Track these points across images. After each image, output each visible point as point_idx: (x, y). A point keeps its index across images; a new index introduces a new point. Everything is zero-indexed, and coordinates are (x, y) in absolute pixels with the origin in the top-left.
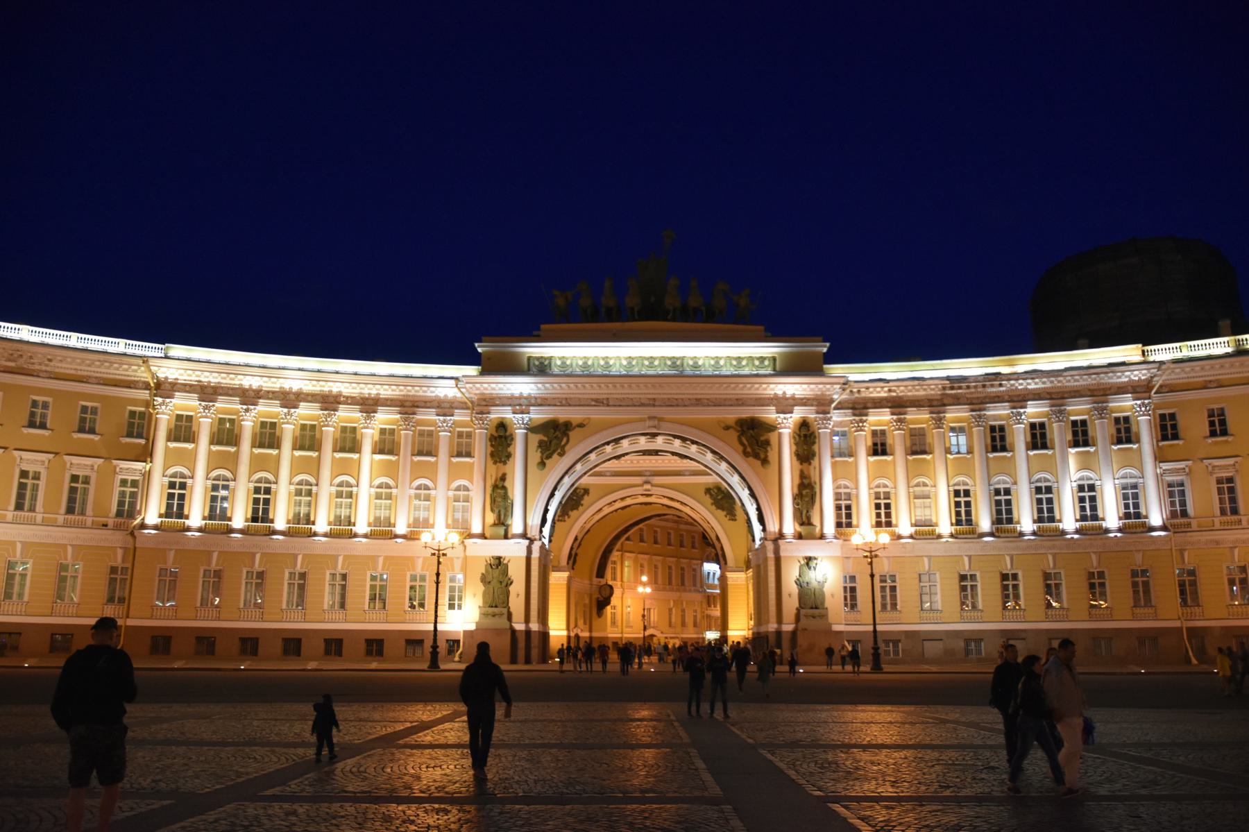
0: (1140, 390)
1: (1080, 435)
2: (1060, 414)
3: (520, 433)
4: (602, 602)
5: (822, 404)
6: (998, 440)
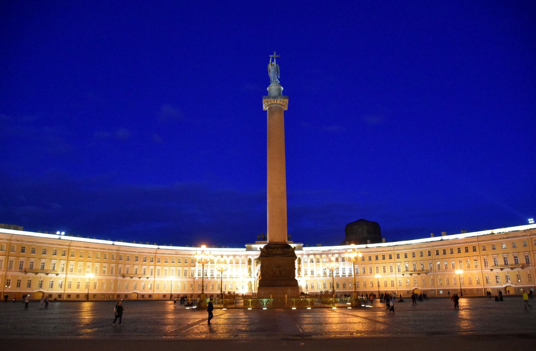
1: (343, 260)
2: (340, 256)
3: (253, 260)
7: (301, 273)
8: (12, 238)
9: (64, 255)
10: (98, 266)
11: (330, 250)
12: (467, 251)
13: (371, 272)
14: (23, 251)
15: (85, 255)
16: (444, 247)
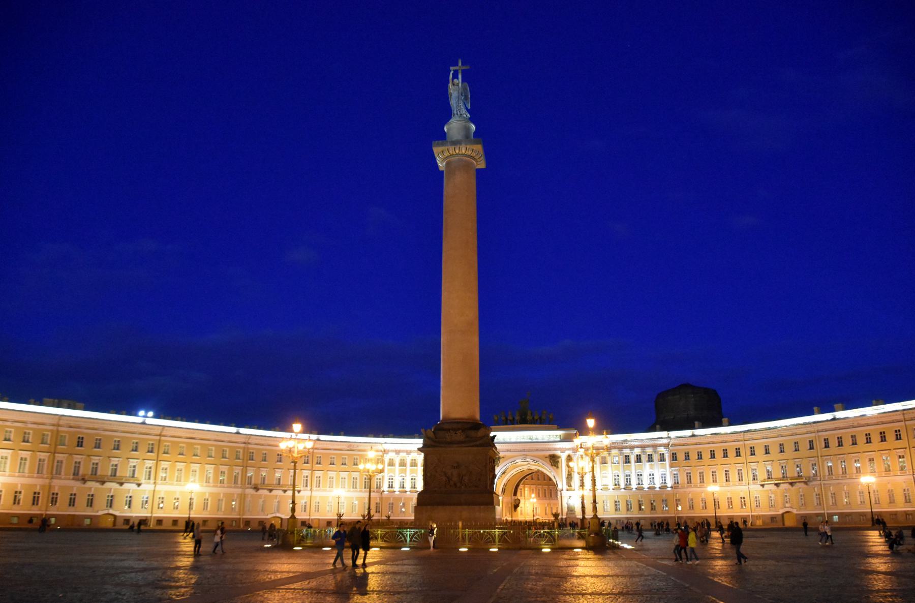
0: (666, 446)
1: (650, 459)
2: (644, 452)
4: (516, 506)
5: (575, 450)
6: (627, 460)
7: (572, 484)
8: (61, 422)
9: (152, 452)
10: (212, 471)
11: (625, 441)
12: (883, 439)
13: (702, 481)
14: (80, 443)
15: (188, 451)
16: (838, 433)
